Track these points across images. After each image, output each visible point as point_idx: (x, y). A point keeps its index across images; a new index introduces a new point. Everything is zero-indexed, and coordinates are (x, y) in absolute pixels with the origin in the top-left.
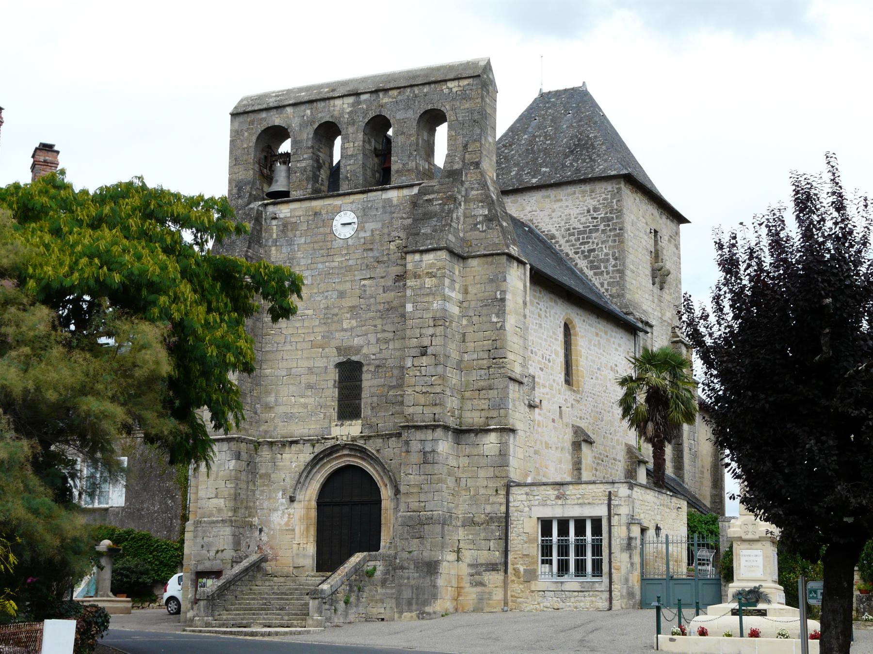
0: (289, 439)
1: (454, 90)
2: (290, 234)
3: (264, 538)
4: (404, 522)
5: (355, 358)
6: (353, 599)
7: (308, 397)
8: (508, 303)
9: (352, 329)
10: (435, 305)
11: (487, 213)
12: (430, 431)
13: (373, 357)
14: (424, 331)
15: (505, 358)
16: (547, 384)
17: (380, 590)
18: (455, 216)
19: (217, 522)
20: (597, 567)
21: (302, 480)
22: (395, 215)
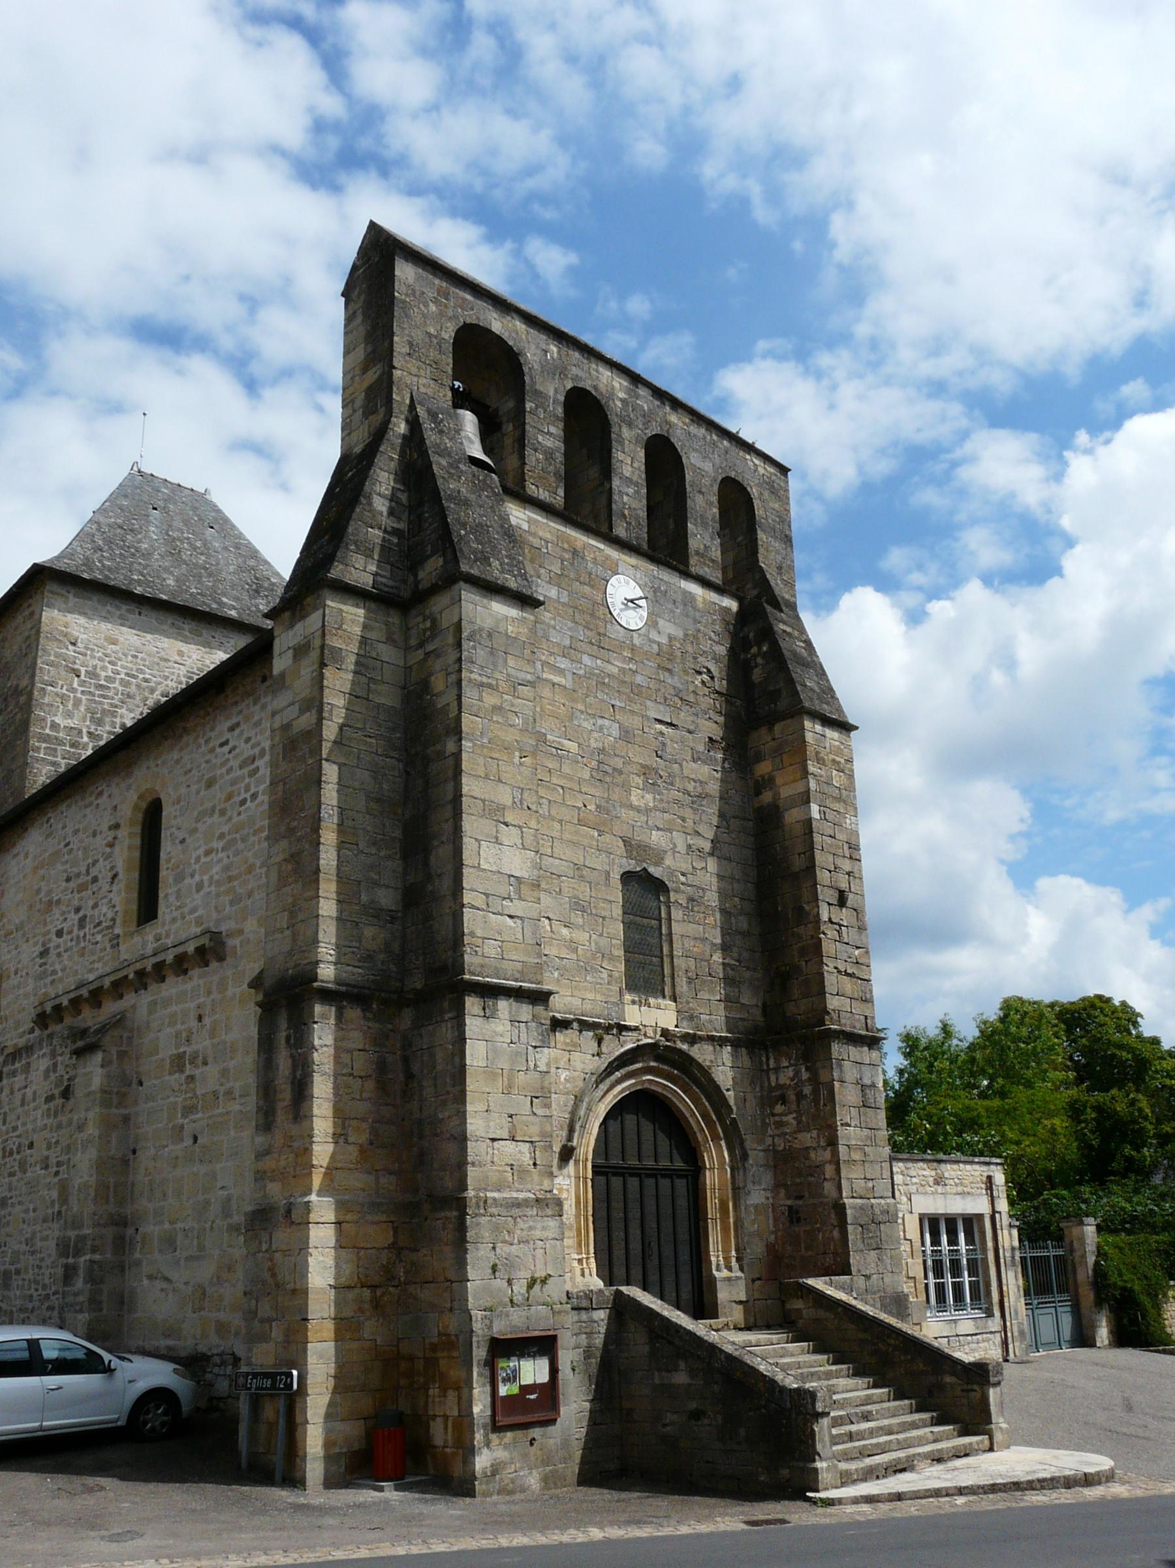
7: (578, 927)
9: (648, 811)
13: (683, 879)
19: (526, 1203)
20: (975, 1296)
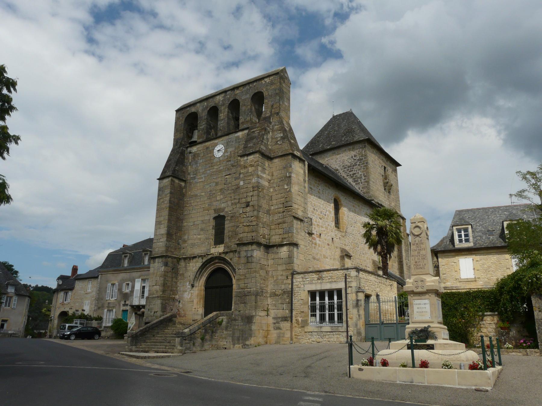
0: (192, 256)
1: (267, 82)
2: (196, 159)
3: (181, 305)
5: (222, 214)
6: (207, 337)
8: (292, 178)
9: (221, 199)
10: (253, 180)
11: (282, 135)
12: (250, 246)
13: (230, 212)
14: (248, 194)
15: (291, 206)
16: (324, 226)
17: (225, 332)
18: (265, 137)
19: (155, 297)
20: (340, 317)
21: (197, 276)
22: (241, 143)
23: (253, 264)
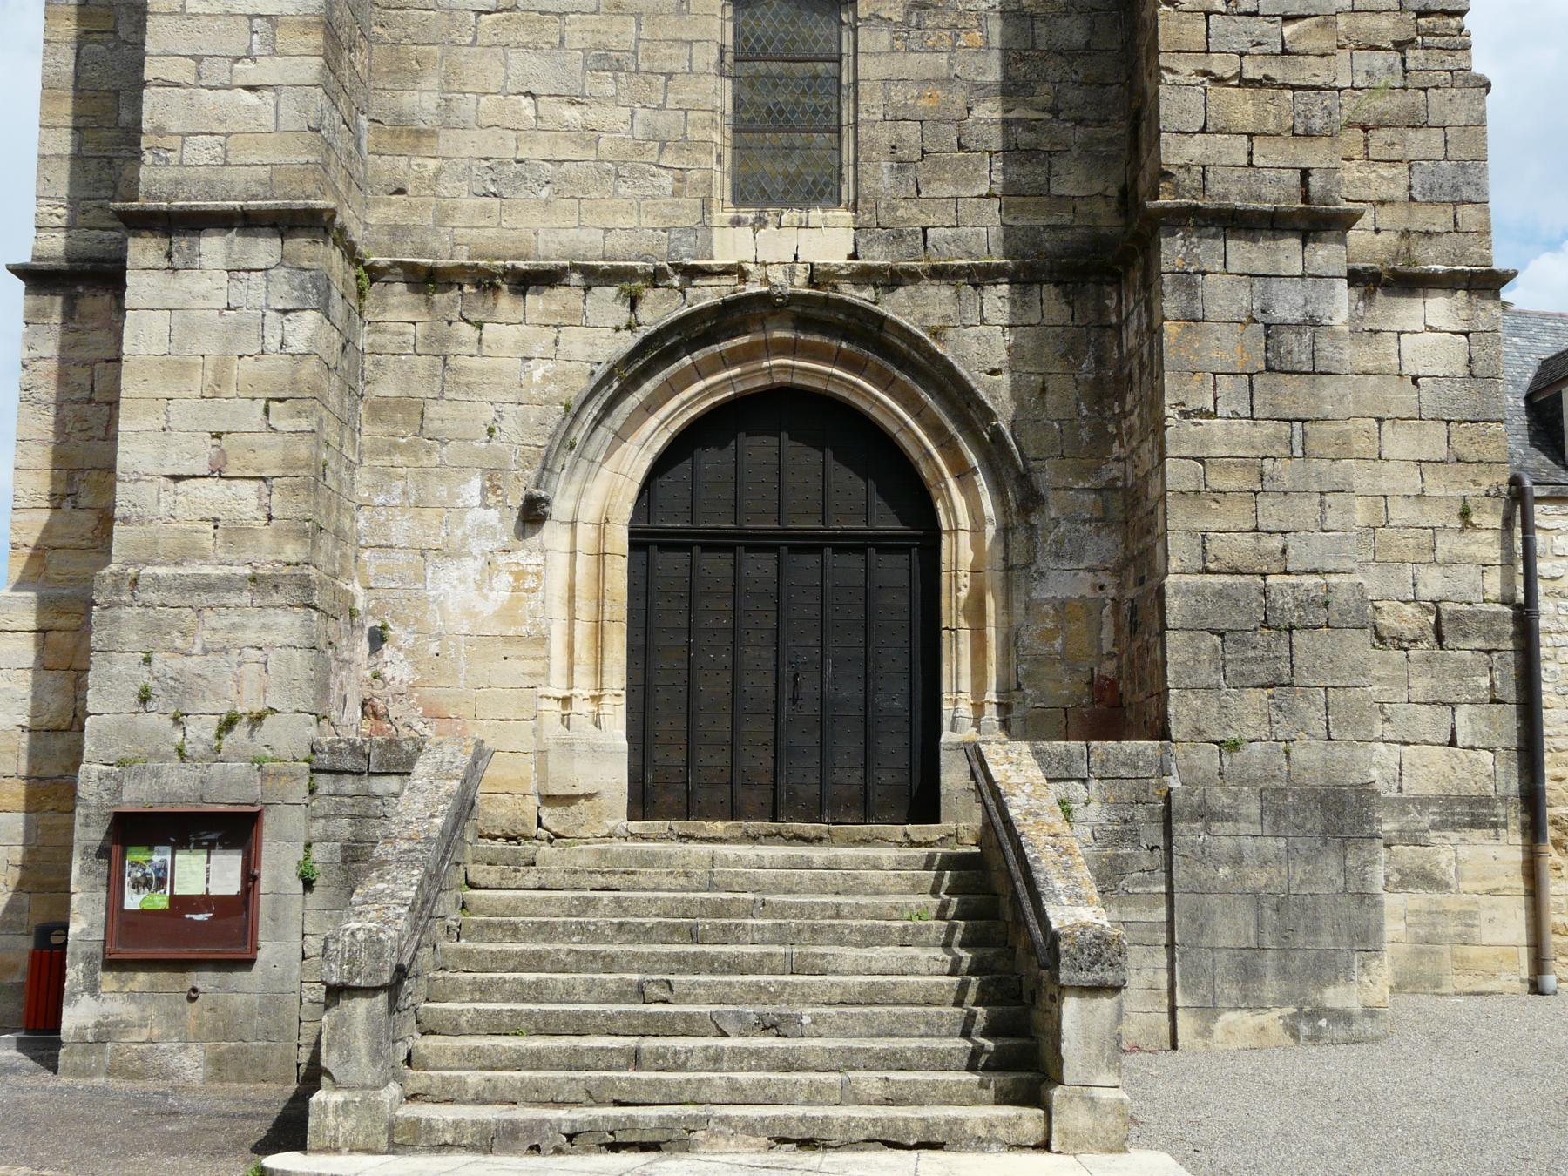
4: (1197, 615)
7: (600, 100)
12: (1292, 243)
19: (228, 584)
21: (578, 435)
23: (1329, 387)
